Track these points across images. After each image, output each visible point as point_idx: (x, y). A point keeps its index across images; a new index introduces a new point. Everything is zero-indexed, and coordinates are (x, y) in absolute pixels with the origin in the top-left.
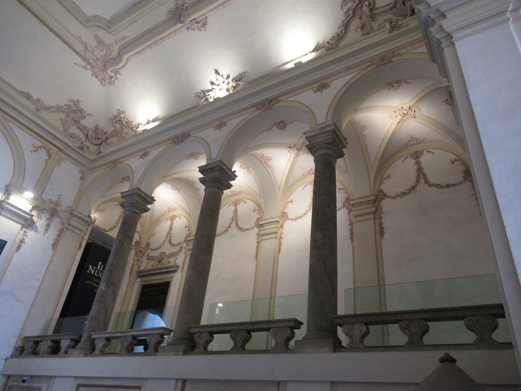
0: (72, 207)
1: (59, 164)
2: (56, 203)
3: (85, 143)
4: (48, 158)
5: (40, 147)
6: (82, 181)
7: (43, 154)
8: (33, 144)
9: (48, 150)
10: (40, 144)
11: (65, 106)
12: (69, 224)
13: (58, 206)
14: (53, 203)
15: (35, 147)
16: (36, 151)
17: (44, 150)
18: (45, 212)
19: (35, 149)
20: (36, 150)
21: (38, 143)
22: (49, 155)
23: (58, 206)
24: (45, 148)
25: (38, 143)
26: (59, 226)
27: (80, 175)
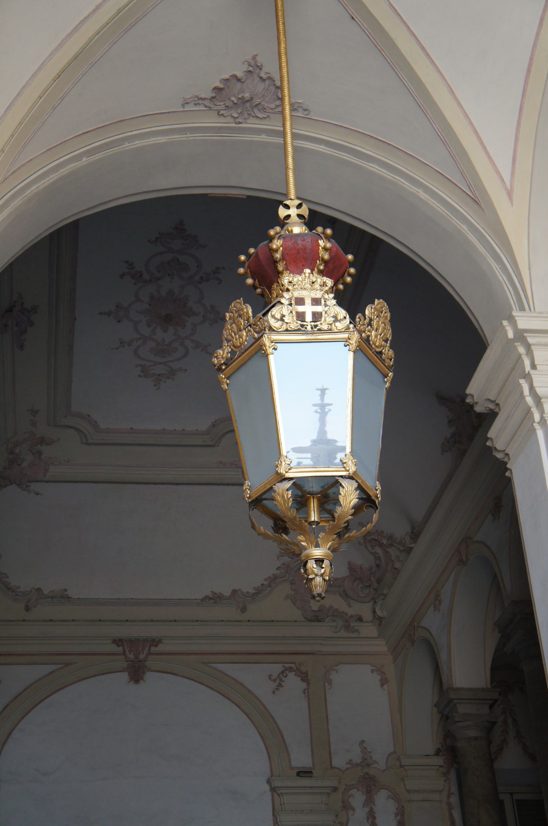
0: (395, 752)
1: (330, 682)
2: (364, 760)
3: (351, 612)
4: (304, 685)
5: (283, 672)
6: (385, 687)
7: (293, 682)
8: (270, 677)
9: (298, 669)
10: (278, 668)
11: (278, 572)
12: (408, 791)
13: (368, 765)
14: (358, 765)
15: (274, 681)
16: (280, 685)
17: (291, 675)
18: (354, 792)
19: (278, 681)
20: (279, 682)
21: (277, 669)
22: (305, 678)
23: (368, 765)
24: (291, 669)
25: (277, 669)
26: (392, 806)
27: (377, 677)
